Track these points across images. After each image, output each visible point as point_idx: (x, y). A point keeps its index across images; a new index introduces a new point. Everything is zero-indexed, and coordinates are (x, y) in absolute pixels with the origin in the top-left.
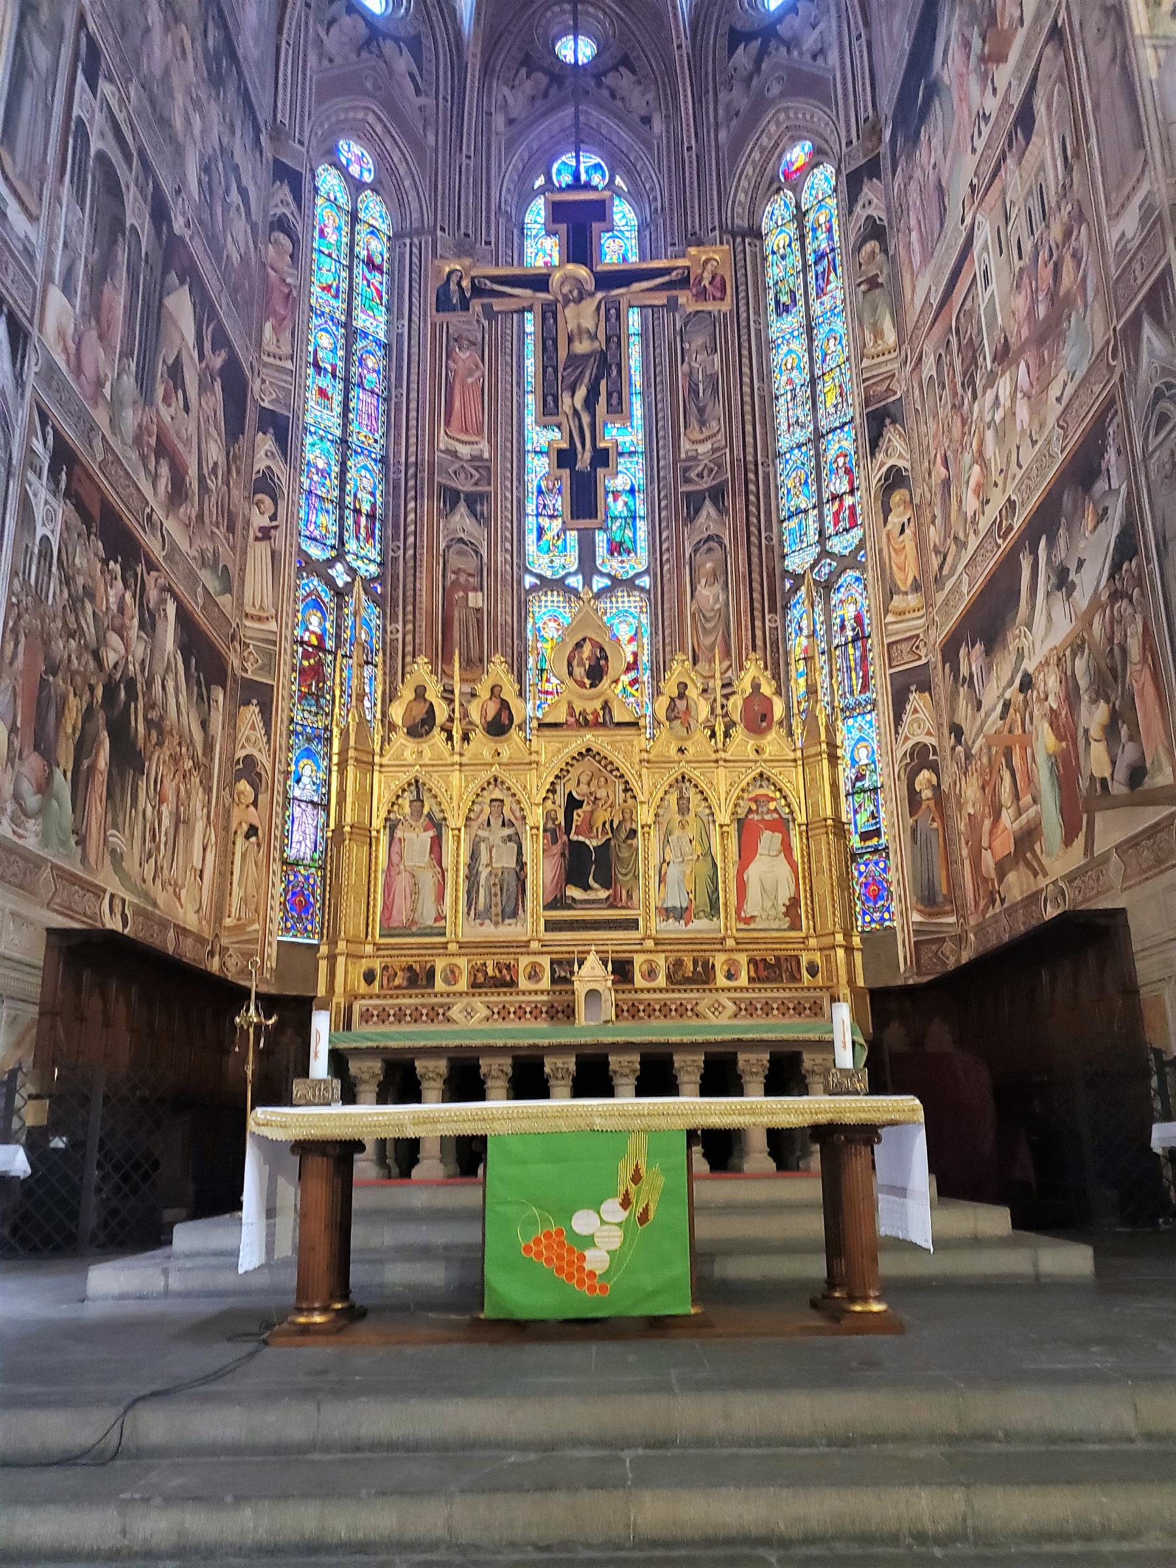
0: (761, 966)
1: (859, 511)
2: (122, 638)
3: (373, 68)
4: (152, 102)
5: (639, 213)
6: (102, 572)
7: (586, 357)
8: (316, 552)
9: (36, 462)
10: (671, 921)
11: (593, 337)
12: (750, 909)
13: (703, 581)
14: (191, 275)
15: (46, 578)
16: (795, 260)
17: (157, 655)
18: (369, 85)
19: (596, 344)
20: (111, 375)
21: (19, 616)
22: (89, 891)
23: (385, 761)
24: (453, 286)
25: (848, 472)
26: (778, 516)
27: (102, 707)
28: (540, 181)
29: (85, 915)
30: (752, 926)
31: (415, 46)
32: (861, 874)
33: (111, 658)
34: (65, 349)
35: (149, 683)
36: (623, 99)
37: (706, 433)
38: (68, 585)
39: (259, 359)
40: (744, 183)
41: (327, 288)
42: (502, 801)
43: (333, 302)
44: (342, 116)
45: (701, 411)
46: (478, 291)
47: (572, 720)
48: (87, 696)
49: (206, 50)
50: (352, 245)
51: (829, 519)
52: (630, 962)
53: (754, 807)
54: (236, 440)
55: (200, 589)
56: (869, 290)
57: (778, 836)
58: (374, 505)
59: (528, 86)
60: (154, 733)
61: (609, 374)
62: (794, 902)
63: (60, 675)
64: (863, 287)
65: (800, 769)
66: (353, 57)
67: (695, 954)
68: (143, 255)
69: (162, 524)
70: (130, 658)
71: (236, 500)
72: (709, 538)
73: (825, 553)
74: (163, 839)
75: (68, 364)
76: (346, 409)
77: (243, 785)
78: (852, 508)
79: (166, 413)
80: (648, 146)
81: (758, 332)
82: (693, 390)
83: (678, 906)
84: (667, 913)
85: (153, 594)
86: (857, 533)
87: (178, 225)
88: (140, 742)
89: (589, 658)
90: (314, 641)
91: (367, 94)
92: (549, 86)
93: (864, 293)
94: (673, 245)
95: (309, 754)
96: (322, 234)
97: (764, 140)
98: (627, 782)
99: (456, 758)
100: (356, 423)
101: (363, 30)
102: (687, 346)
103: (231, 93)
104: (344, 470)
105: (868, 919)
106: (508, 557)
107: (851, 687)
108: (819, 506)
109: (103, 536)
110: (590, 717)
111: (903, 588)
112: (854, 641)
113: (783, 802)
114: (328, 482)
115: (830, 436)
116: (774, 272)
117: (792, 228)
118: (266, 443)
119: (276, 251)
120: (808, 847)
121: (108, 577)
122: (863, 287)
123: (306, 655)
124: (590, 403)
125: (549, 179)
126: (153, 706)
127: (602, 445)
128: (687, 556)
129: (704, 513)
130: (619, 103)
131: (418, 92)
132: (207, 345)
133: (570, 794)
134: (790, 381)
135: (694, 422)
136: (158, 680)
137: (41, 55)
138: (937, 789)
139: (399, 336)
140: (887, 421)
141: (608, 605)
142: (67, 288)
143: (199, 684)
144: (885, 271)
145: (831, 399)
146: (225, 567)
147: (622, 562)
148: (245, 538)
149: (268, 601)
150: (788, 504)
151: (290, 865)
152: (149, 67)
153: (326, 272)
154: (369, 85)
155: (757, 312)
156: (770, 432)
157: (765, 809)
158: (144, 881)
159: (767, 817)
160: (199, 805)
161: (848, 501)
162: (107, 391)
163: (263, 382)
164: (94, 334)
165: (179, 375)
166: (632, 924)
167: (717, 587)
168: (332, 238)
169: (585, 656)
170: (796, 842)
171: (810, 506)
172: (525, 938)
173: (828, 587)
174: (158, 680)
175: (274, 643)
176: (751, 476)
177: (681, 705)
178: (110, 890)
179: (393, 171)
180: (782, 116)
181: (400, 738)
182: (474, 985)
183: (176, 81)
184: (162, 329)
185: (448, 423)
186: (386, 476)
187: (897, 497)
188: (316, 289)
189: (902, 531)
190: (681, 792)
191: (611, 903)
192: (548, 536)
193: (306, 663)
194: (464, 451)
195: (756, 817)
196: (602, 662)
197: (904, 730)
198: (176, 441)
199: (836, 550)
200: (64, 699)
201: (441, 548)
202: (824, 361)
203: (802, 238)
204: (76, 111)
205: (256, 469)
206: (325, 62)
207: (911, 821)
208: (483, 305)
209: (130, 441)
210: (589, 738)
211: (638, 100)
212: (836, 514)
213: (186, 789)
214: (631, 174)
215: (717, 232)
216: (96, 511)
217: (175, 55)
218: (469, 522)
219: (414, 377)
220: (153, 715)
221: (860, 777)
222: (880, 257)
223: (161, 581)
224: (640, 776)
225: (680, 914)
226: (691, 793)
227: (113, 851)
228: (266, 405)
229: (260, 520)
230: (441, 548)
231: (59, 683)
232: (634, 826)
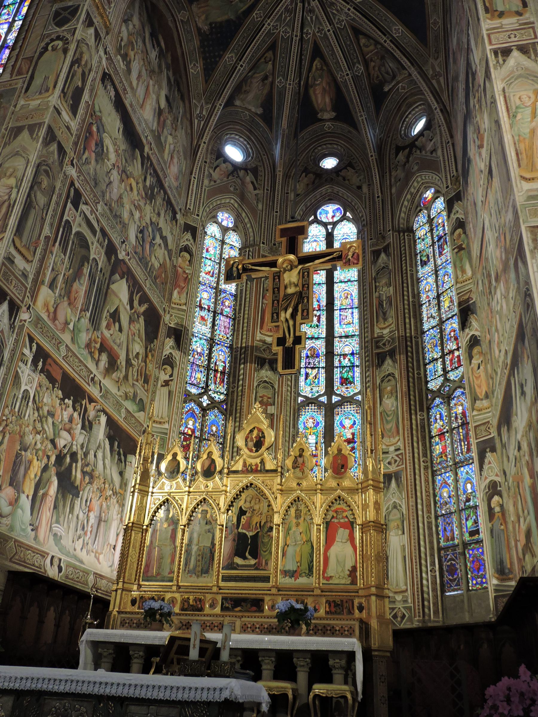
0: (333, 605)
1: (461, 358)
2: (70, 433)
3: (234, 182)
4: (111, 210)
5: (358, 228)
6: (60, 404)
7: (293, 294)
8: (194, 391)
9: (25, 358)
10: (287, 578)
11: (296, 286)
12: (330, 572)
13: (386, 396)
14: (129, 275)
15: (25, 408)
16: (429, 240)
17: (92, 440)
18: (232, 189)
19: (298, 289)
20: (74, 319)
21: (7, 425)
22: (37, 553)
23: (155, 490)
24: (235, 269)
25: (456, 339)
26: (424, 362)
27: (54, 465)
28: (312, 217)
29: (34, 565)
30: (330, 582)
31: (255, 171)
32: (470, 555)
33: (61, 443)
34: (48, 310)
35: (86, 454)
36: (348, 180)
37: (387, 324)
38: (38, 410)
39: (169, 306)
40: (404, 209)
41: (208, 273)
42: (207, 511)
43: (211, 279)
44: (219, 202)
45: (384, 314)
46: (245, 270)
47: (245, 469)
48: (45, 460)
49: (145, 186)
50: (221, 255)
51: (448, 363)
52: (262, 600)
53: (335, 515)
54: (153, 342)
55: (123, 410)
56: (459, 251)
57: (347, 531)
58: (224, 367)
59: (306, 180)
60: (87, 479)
61: (303, 302)
62: (354, 569)
63: (29, 450)
64: (456, 250)
65: (360, 494)
66: (225, 179)
67: (297, 597)
68: (99, 269)
69: (100, 382)
70: (74, 443)
71: (150, 369)
72: (389, 375)
73: (447, 380)
74: (90, 529)
75: (49, 316)
78: (458, 357)
79: (107, 333)
80: (360, 198)
81: (412, 275)
82: (381, 304)
83: (292, 569)
84: (285, 573)
85: (92, 413)
86: (461, 369)
87: (122, 255)
88: (78, 482)
89: (256, 437)
90: (190, 432)
91: (230, 192)
92: (315, 179)
93: (457, 253)
94: (371, 239)
96: (207, 251)
97: (412, 190)
98: (269, 501)
99: (187, 489)
100: (218, 331)
101: (230, 168)
102: (378, 284)
103: (159, 200)
105: (474, 582)
106: (289, 389)
107: (461, 449)
108: (443, 356)
109: (60, 389)
110: (254, 467)
111: (480, 397)
112: (463, 424)
113: (351, 512)
114: (202, 358)
115: (447, 322)
116: (420, 246)
117: (427, 228)
118: (170, 342)
119: (182, 261)
120: (362, 537)
121: (64, 406)
122: (456, 250)
123: (185, 440)
124: (293, 316)
125: (316, 217)
126: (87, 465)
127: (297, 334)
128: (378, 384)
129: (386, 362)
130: (347, 182)
131: (255, 189)
132: (136, 303)
133: (241, 507)
134: (428, 297)
135: (381, 319)
136: (92, 453)
137: (41, 200)
138: (502, 506)
139: (242, 290)
140: (470, 313)
141: (340, 410)
142: (52, 286)
143: (119, 454)
144: (466, 242)
145: (447, 304)
146: (141, 400)
147: (347, 388)
148: (155, 386)
149: (165, 415)
150: (429, 356)
152: (110, 196)
153: (208, 266)
154: (232, 189)
155: (411, 266)
157: (341, 517)
158: (75, 550)
159: (342, 521)
160: (115, 513)
161: (456, 353)
162: (71, 326)
163: (171, 315)
164: (66, 303)
165: (117, 316)
166: (266, 579)
167: (393, 399)
169: (254, 436)
170: (357, 534)
171: (439, 356)
172: (211, 585)
173: (448, 398)
174: (92, 453)
175: (166, 434)
176: (409, 343)
177: (299, 459)
178: (52, 554)
179: (242, 222)
180: (419, 179)
182: (182, 609)
183: (125, 200)
184: (108, 299)
185: (261, 328)
186: (232, 353)
187: (476, 350)
188: (203, 274)
189: (479, 368)
190: (297, 507)
191: (256, 567)
192: (311, 377)
193: (185, 443)
195: (335, 521)
196: (262, 439)
197: (485, 473)
198: (112, 344)
199: (452, 378)
200: (30, 462)
201: (255, 386)
202: (443, 286)
203: (431, 230)
204: (65, 218)
205: (164, 354)
206: (212, 183)
207: (490, 525)
208: (247, 276)
209: (83, 346)
210: (251, 478)
211: (355, 180)
212: (451, 360)
213: (107, 506)
214: (353, 212)
215: (391, 232)
216: (59, 378)
217: (126, 190)
218: (269, 373)
219: (247, 308)
220: (88, 469)
221: (468, 500)
222: (463, 236)
223: (98, 407)
224: (276, 498)
225: (293, 574)
226: (302, 507)
227: (55, 535)
228: (172, 325)
229: (164, 377)
230: (255, 386)
231: (28, 455)
232: (272, 525)
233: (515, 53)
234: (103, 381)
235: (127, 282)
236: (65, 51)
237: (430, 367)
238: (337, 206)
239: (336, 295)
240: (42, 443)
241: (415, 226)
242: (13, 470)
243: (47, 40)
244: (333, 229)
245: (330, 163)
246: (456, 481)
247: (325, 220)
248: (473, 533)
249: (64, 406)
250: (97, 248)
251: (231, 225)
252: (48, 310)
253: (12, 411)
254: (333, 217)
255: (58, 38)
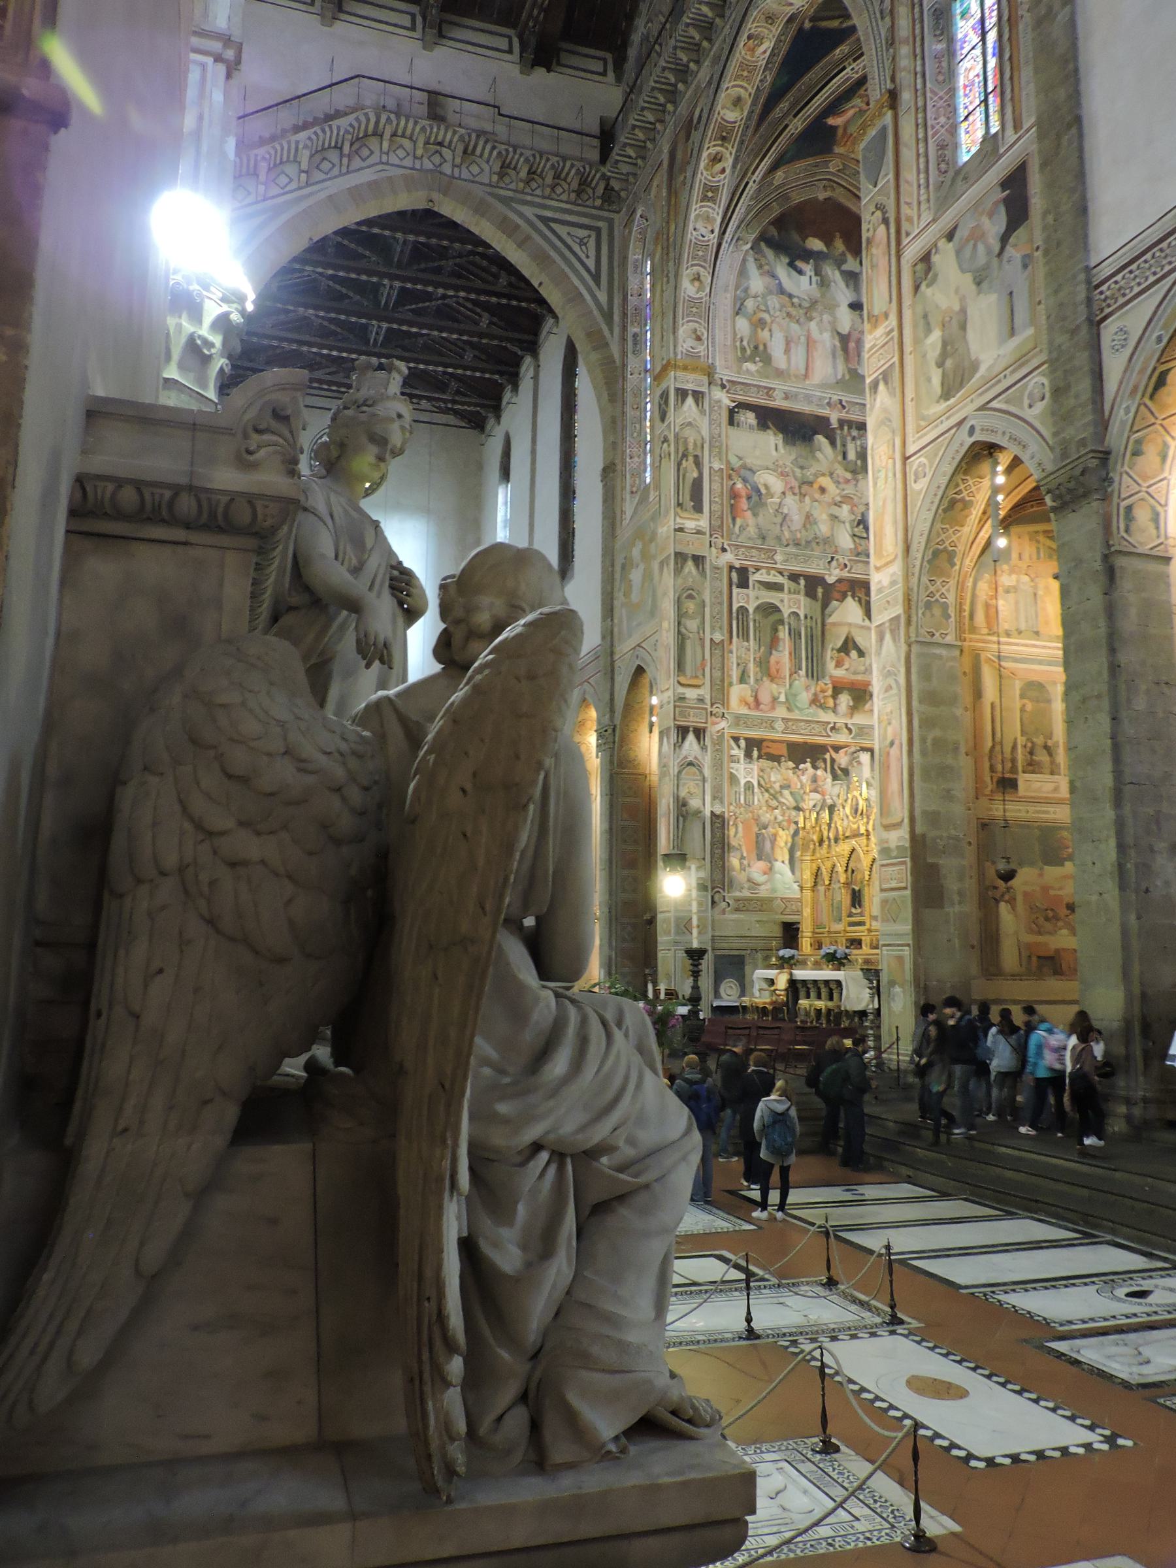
38: (767, 791)
79: (839, 673)
162: (782, 698)
200: (775, 835)
234: (849, 722)
235: (853, 597)
240: (783, 815)
242: (758, 848)
249: (800, 773)
250: (790, 600)
252: (747, 704)
253: (739, 806)
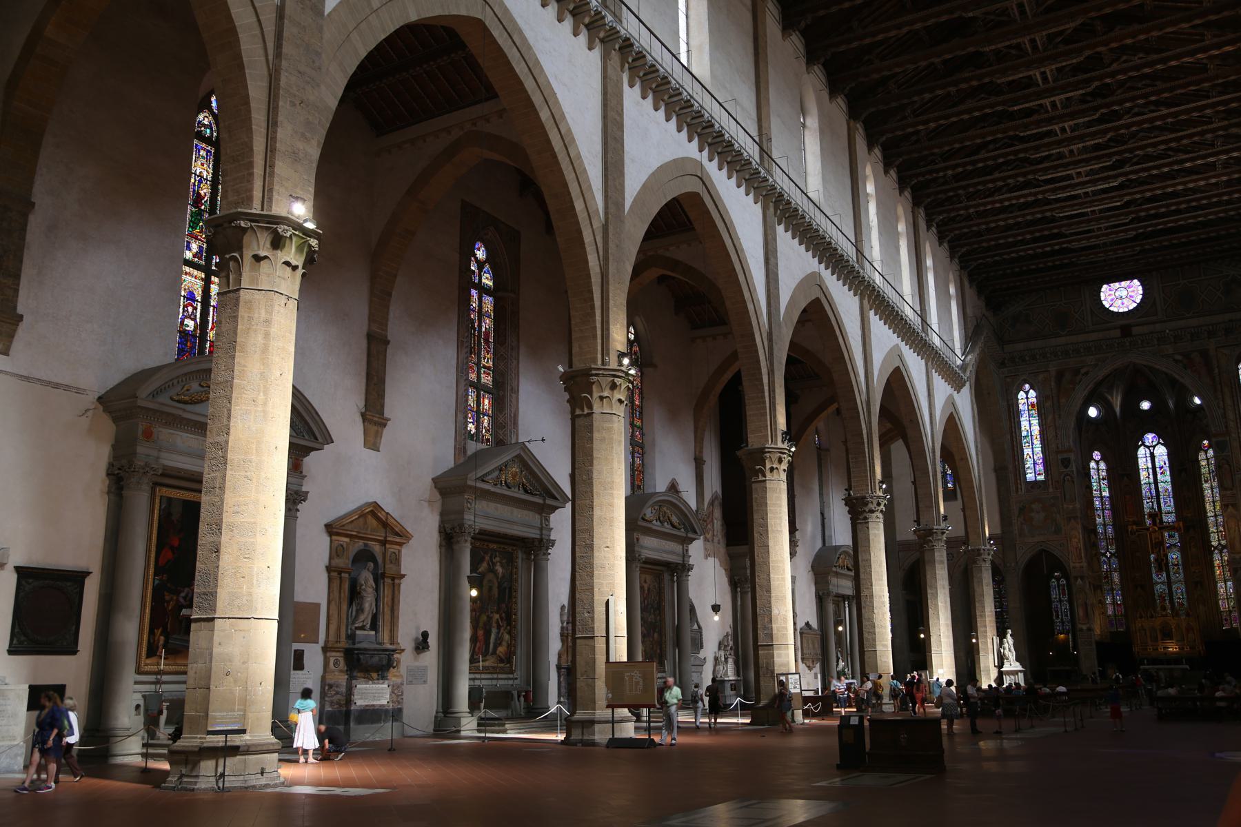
8: (1103, 551)
16: (1207, 469)
28: (1140, 443)
50: (1099, 477)
73: (1220, 544)
76: (1103, 516)
77: (1100, 605)
95: (1108, 594)
104: (1105, 530)
108: (1217, 532)
118: (1093, 536)
151: (1109, 616)
156: (1205, 512)
168: (1095, 477)
173: (1221, 552)
181: (1139, 619)
194: (1131, 520)
212: (1221, 535)
229: (1094, 552)
233: (1230, 507)
236: (1073, 482)
237: (1212, 535)
238: (1154, 435)
239: (1160, 490)
241: (1200, 458)
243: (1063, 475)
244: (1154, 450)
245: (1145, 405)
246: (1226, 587)
247: (1147, 444)
248: (1233, 608)
251: (1099, 457)
254: (1152, 442)
255: (1067, 475)
